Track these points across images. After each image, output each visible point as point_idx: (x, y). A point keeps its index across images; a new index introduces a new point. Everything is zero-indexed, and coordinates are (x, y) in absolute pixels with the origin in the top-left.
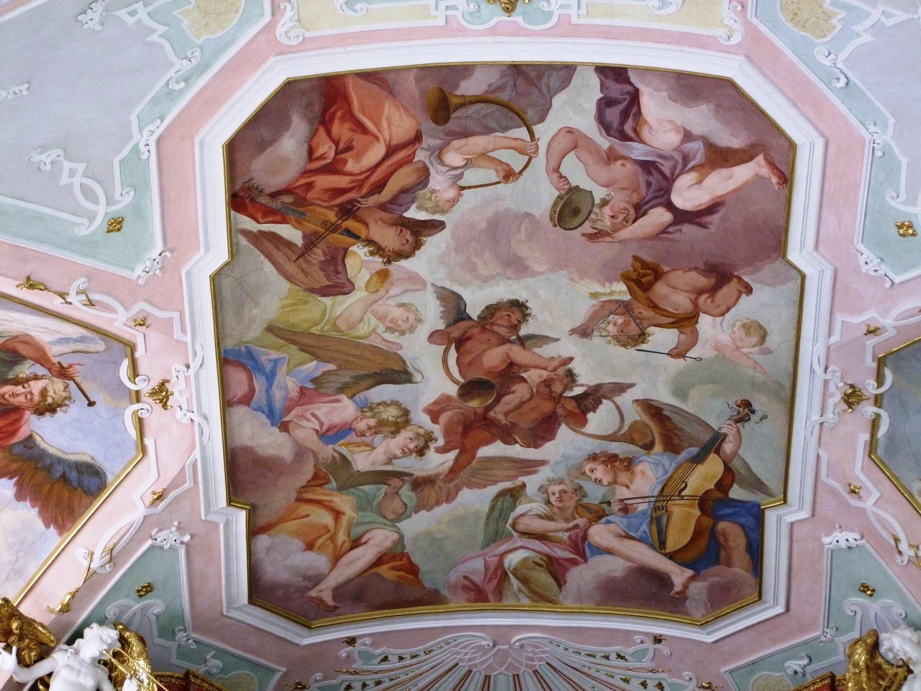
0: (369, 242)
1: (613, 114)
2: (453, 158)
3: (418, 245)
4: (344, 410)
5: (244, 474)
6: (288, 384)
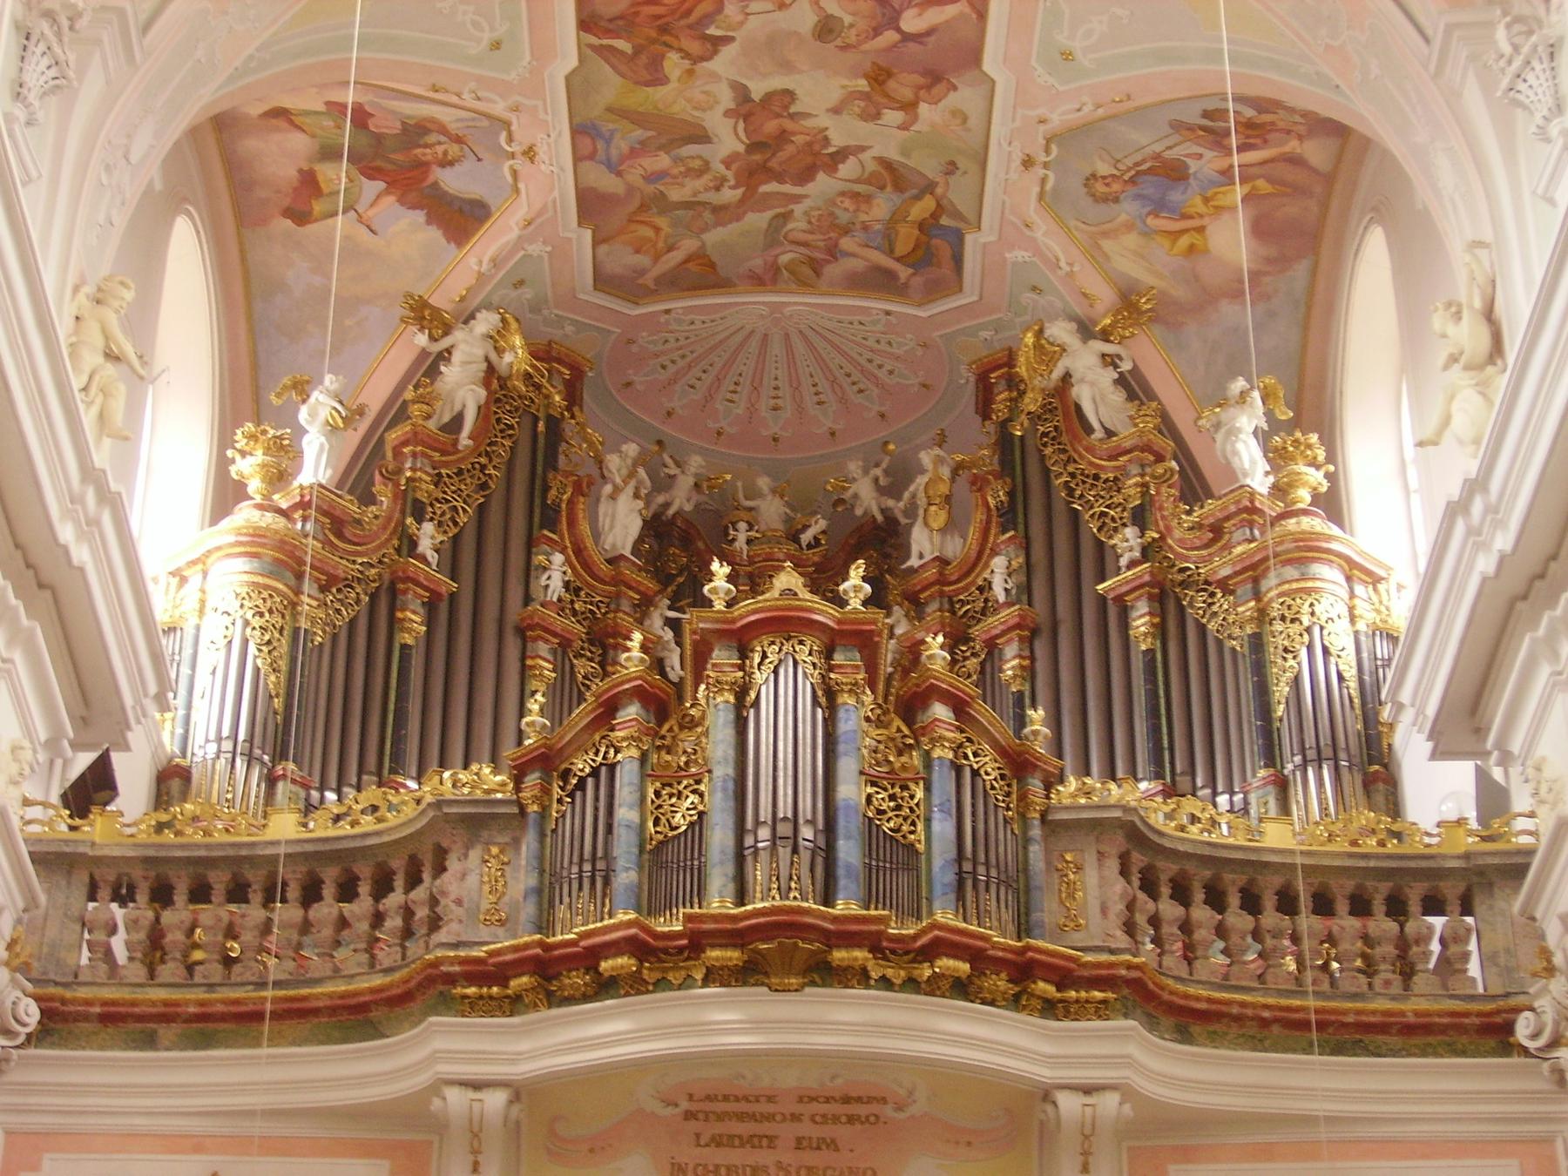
0: (680, 50)
3: (715, 52)
4: (663, 161)
5: (590, 205)
6: (621, 145)
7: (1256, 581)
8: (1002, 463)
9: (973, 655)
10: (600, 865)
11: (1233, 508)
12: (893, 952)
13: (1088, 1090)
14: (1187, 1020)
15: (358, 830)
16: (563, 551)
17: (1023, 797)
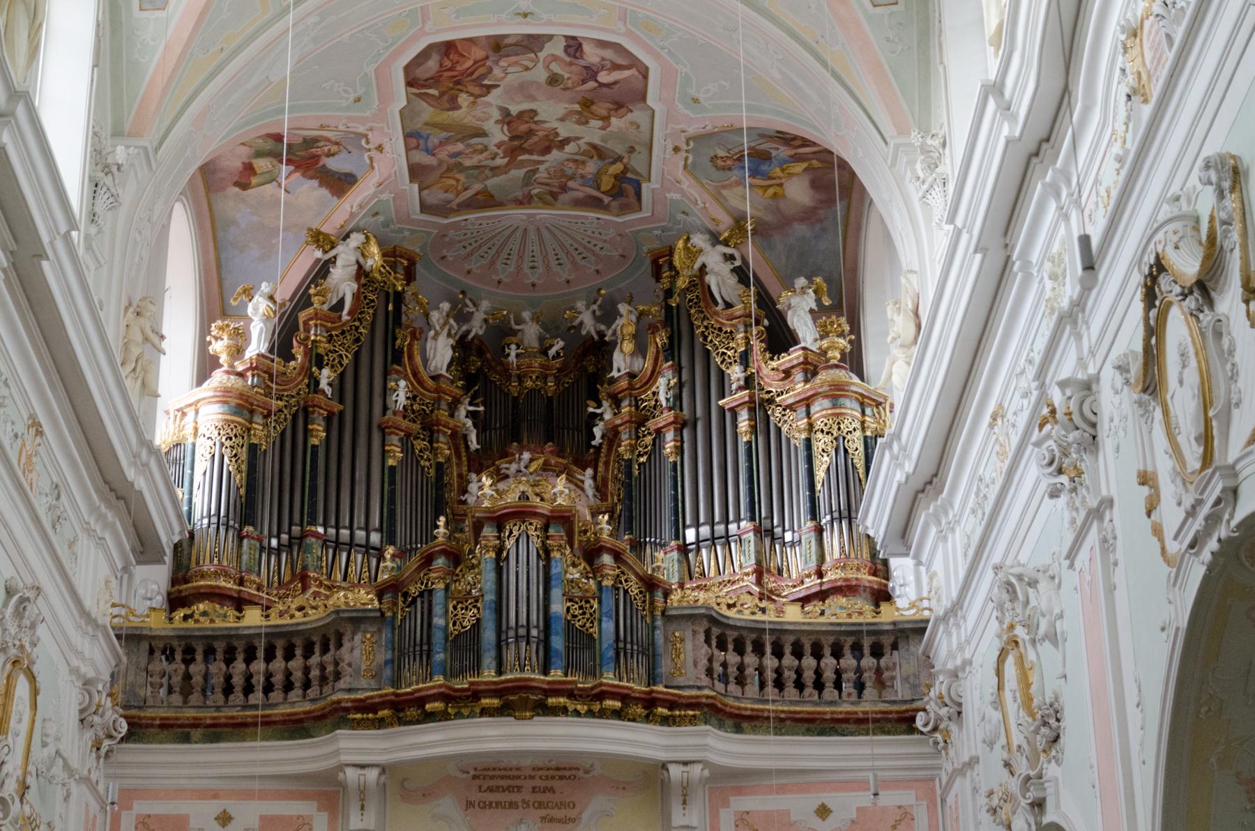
1: (571, 51)
2: (503, 63)
4: (460, 147)
5: (416, 172)
6: (434, 140)
7: (808, 407)
8: (666, 316)
9: (650, 434)
10: (425, 647)
11: (795, 362)
12: (580, 696)
13: (685, 763)
14: (740, 721)
15: (293, 621)
16: (406, 378)
17: (652, 602)
